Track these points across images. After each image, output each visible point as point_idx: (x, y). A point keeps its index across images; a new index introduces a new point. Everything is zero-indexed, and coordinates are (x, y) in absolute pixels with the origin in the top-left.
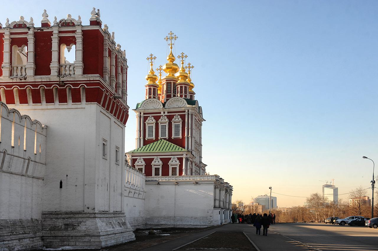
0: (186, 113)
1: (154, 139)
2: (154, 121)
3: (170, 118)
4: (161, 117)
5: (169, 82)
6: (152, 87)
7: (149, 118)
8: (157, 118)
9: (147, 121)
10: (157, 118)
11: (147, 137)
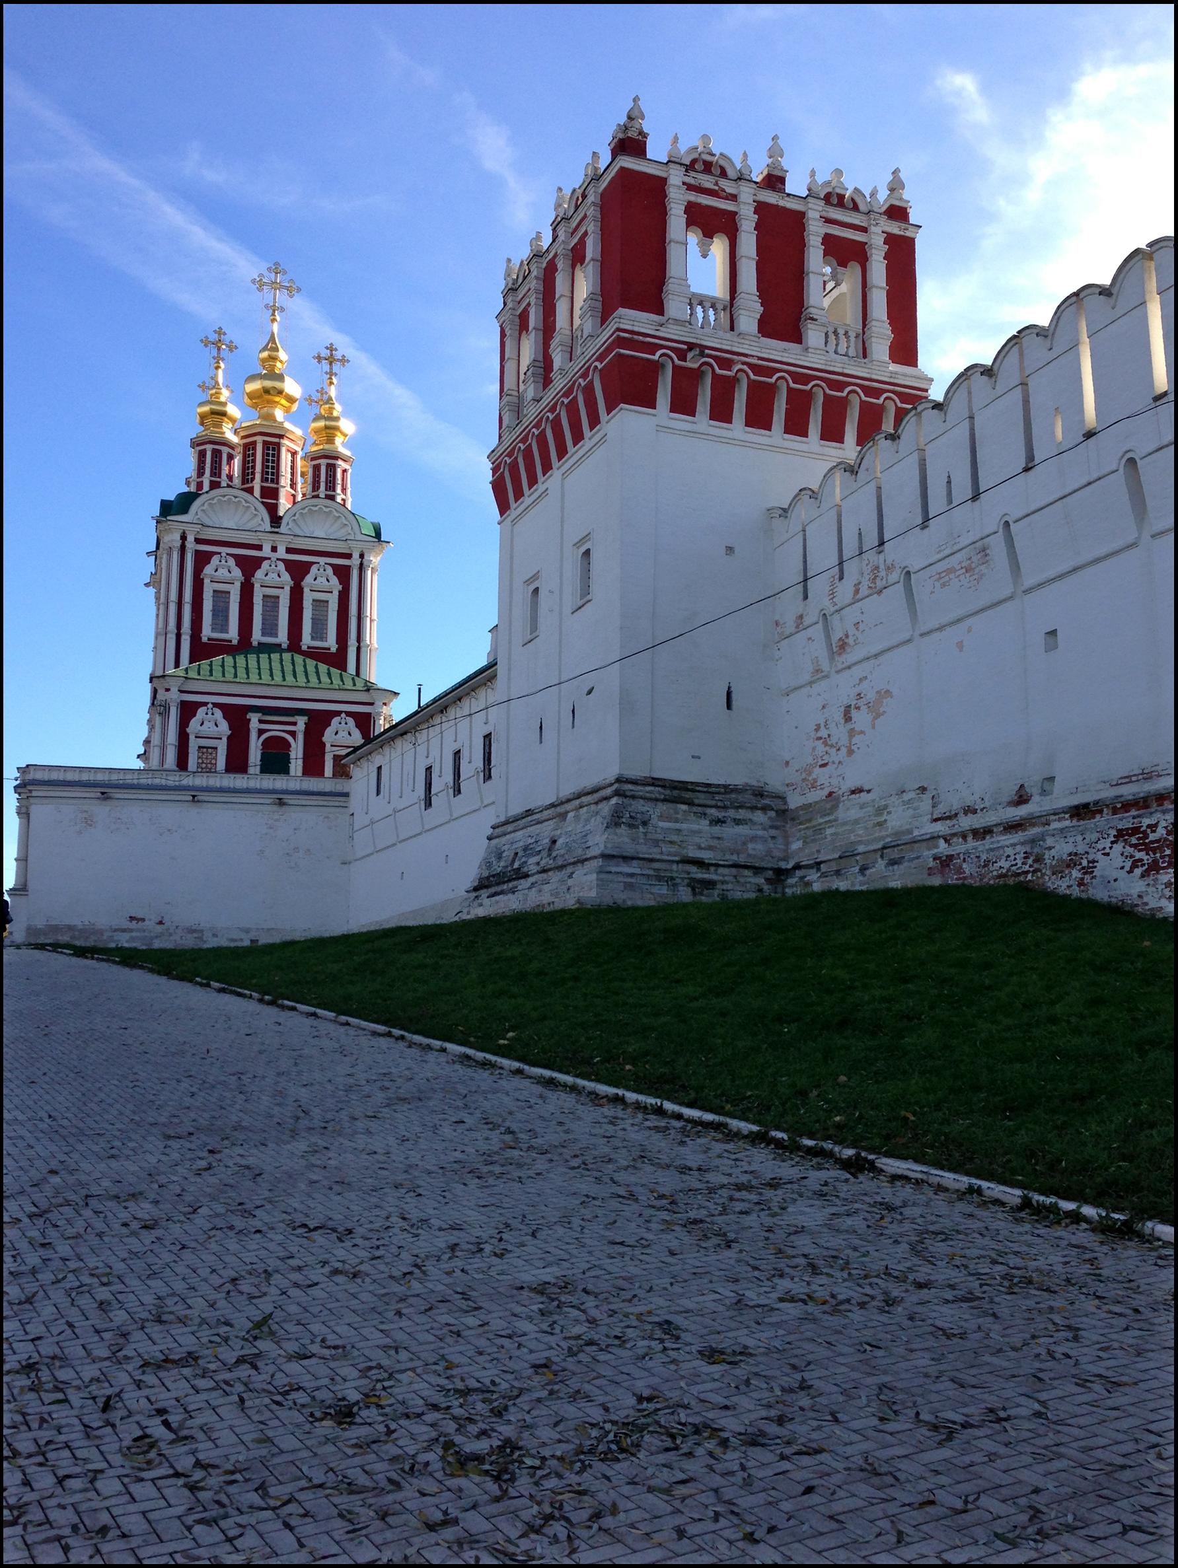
0: (355, 561)
1: (235, 642)
2: (237, 573)
3: (298, 571)
4: (265, 565)
5: (271, 443)
6: (209, 447)
7: (215, 560)
8: (249, 566)
9: (208, 570)
10: (249, 566)
11: (207, 632)
